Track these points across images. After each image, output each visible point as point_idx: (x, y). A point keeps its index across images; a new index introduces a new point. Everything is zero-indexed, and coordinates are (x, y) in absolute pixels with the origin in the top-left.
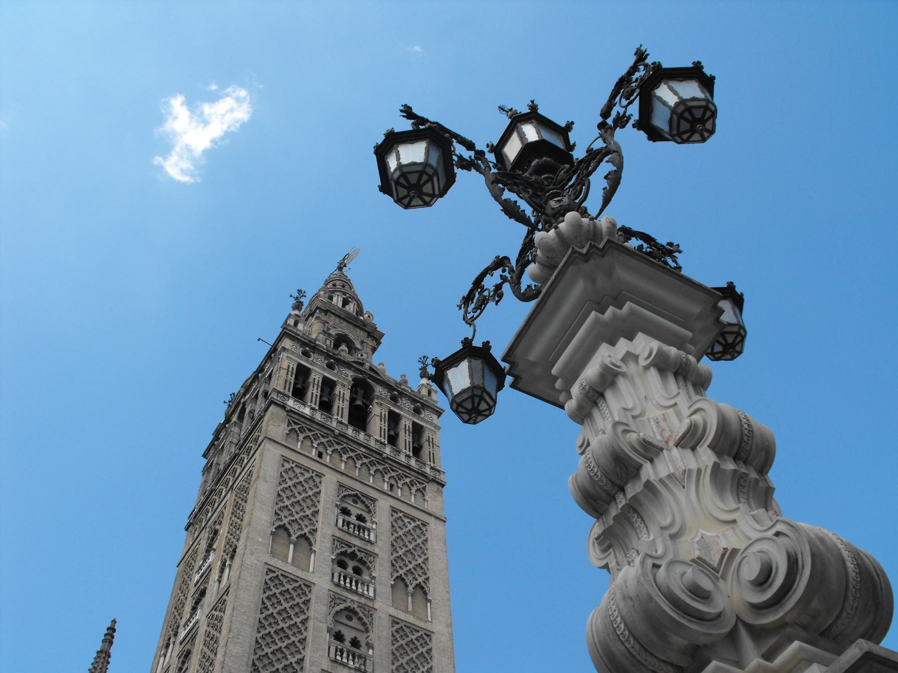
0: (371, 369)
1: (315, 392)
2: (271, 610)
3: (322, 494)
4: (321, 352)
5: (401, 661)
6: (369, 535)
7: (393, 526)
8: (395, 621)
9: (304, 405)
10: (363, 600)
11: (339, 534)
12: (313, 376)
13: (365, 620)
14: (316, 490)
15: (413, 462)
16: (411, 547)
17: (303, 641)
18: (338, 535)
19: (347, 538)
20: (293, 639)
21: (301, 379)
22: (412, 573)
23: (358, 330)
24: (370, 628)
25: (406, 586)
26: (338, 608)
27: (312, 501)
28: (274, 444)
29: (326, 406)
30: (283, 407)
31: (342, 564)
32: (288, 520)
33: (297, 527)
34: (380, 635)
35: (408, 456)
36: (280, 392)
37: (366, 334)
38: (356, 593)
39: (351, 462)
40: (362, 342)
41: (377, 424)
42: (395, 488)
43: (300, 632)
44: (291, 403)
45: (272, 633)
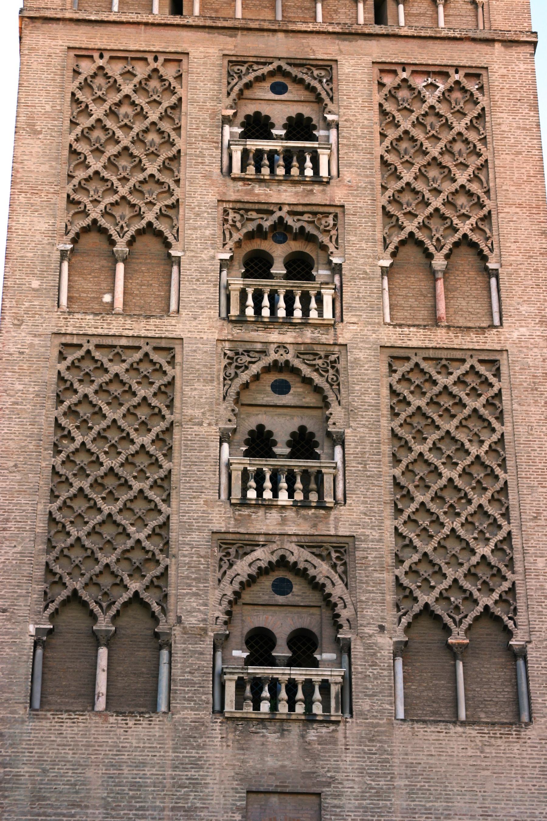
2: (79, 439)
5: (418, 448)
7: (383, 113)
8: (396, 356)
11: (235, 192)
13: (317, 379)
14: (168, 101)
17: (164, 484)
18: (233, 197)
19: (261, 193)
20: (137, 485)
22: (444, 218)
24: (331, 398)
25: (430, 256)
26: (245, 377)
27: (161, 132)
28: (47, 27)
31: (257, 266)
33: (128, 213)
38: (288, 321)
45: (88, 491)
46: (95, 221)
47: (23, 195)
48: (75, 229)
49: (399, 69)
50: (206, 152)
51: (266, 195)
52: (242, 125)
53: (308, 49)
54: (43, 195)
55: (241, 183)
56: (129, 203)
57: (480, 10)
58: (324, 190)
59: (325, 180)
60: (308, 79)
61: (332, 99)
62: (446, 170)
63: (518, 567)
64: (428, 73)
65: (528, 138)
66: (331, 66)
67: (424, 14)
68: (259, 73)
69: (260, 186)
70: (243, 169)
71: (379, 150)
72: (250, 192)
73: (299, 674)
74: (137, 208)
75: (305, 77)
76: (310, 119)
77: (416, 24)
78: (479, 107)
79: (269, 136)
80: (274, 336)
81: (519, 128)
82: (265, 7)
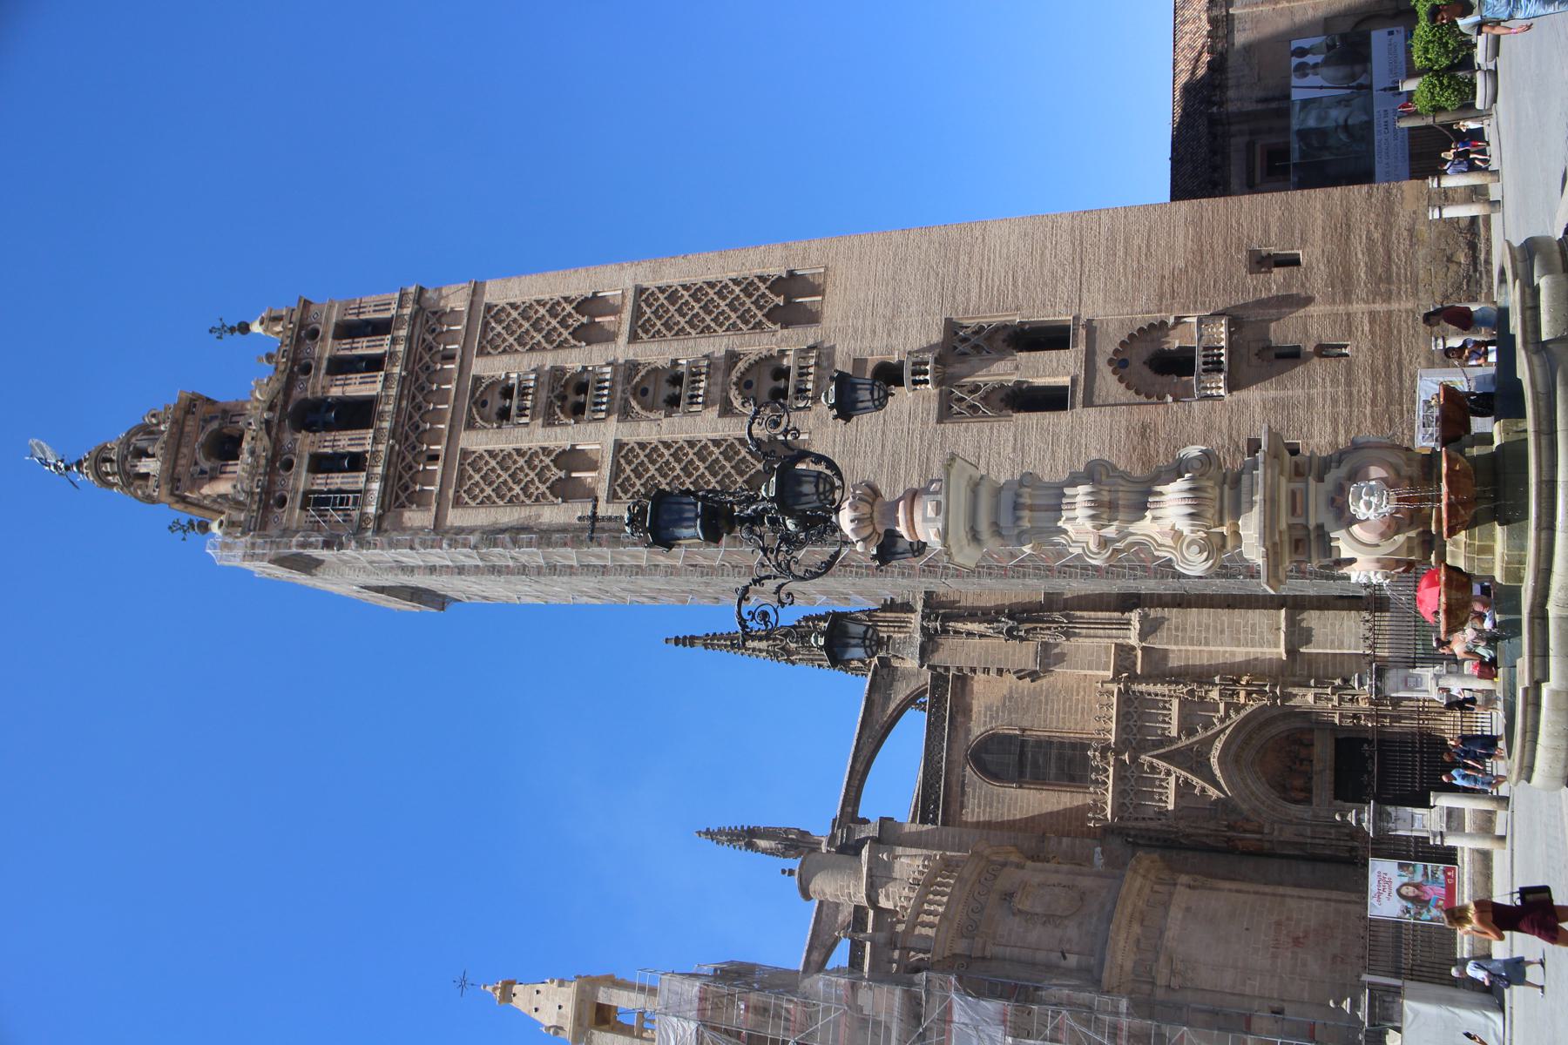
0: (271, 408)
3: (490, 447)
4: (271, 482)
7: (504, 351)
8: (634, 338)
10: (619, 378)
16: (526, 325)
17: (691, 444)
23: (187, 429)
26: (637, 408)
29: (356, 462)
30: (379, 518)
34: (656, 354)
35: (394, 341)
40: (207, 421)
41: (357, 387)
43: (681, 448)
48: (551, 498)
63: (746, 273)
73: (793, 374)
79: (509, 409)
80: (619, 395)
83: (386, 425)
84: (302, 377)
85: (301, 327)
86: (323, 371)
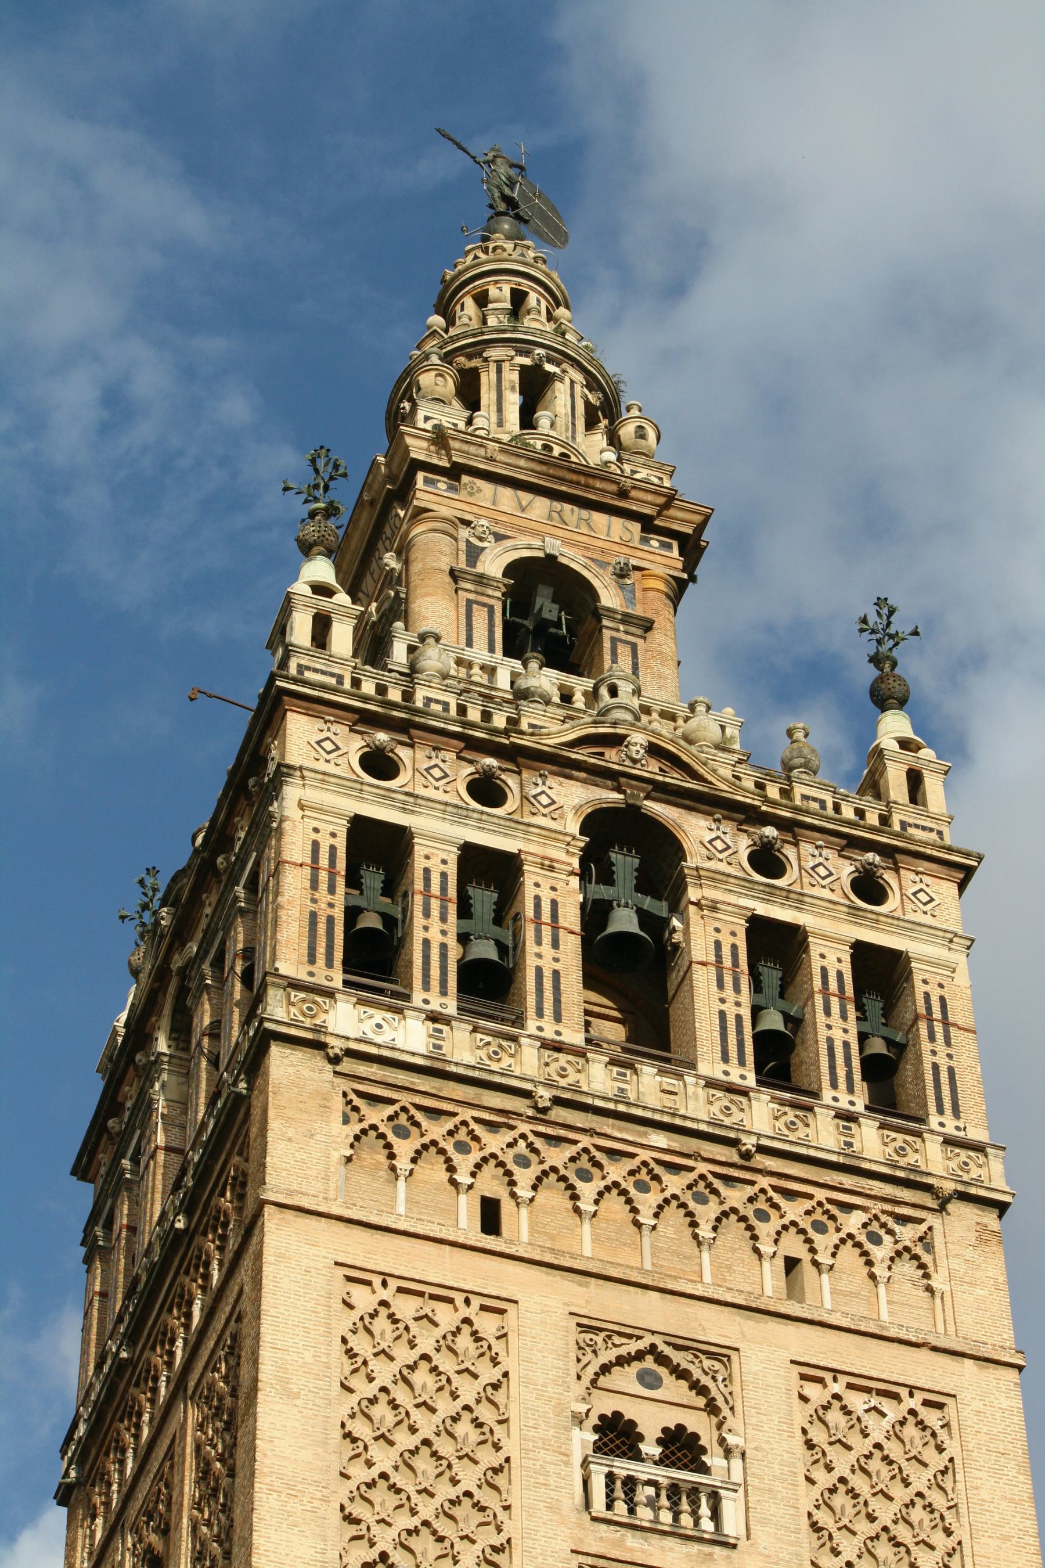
0: (654, 750)
1: (435, 936)
6: (716, 1515)
7: (810, 1445)
9: (399, 1011)
12: (420, 849)
14: (489, 1374)
15: (871, 1141)
16: (886, 1513)
21: (373, 879)
23: (600, 519)
29: (489, 986)
32: (392, 1533)
35: (848, 1117)
36: (295, 985)
37: (636, 527)
39: (614, 1203)
40: (622, 573)
41: (714, 1002)
42: (807, 1269)
44: (347, 1019)
46: (384, 1556)
47: (275, 1494)
49: (828, 1377)
50: (551, 1468)
51: (643, 1552)
52: (596, 1429)
53: (695, 1324)
54: (305, 1500)
55: (603, 1527)
56: (434, 1532)
57: (938, 1301)
58: (728, 1557)
59: (732, 1541)
60: (697, 1374)
61: (732, 1409)
62: (902, 1549)
64: (868, 1390)
65: (1018, 1515)
66: (729, 1357)
67: (857, 1295)
68: (623, 1351)
69: (633, 1536)
70: (609, 1507)
71: (807, 1505)
72: (620, 1544)
74: (447, 1543)
75: (691, 1368)
76: (695, 1437)
77: (845, 1309)
78: (946, 1456)
79: (637, 1456)
81: (1004, 1498)
82: (625, 1245)
83: (598, 1079)
84: (743, 846)
85: (888, 852)
86: (763, 909)
